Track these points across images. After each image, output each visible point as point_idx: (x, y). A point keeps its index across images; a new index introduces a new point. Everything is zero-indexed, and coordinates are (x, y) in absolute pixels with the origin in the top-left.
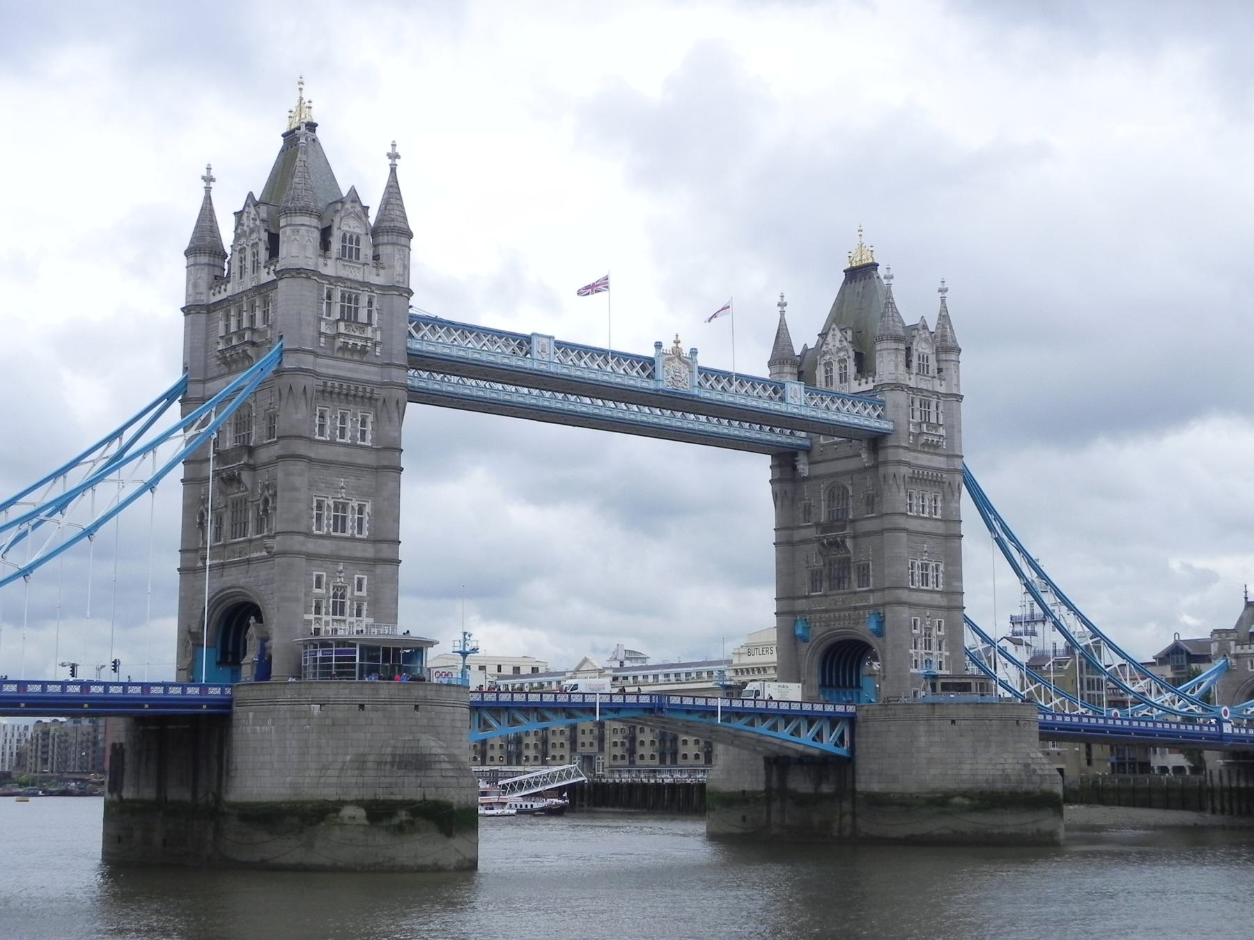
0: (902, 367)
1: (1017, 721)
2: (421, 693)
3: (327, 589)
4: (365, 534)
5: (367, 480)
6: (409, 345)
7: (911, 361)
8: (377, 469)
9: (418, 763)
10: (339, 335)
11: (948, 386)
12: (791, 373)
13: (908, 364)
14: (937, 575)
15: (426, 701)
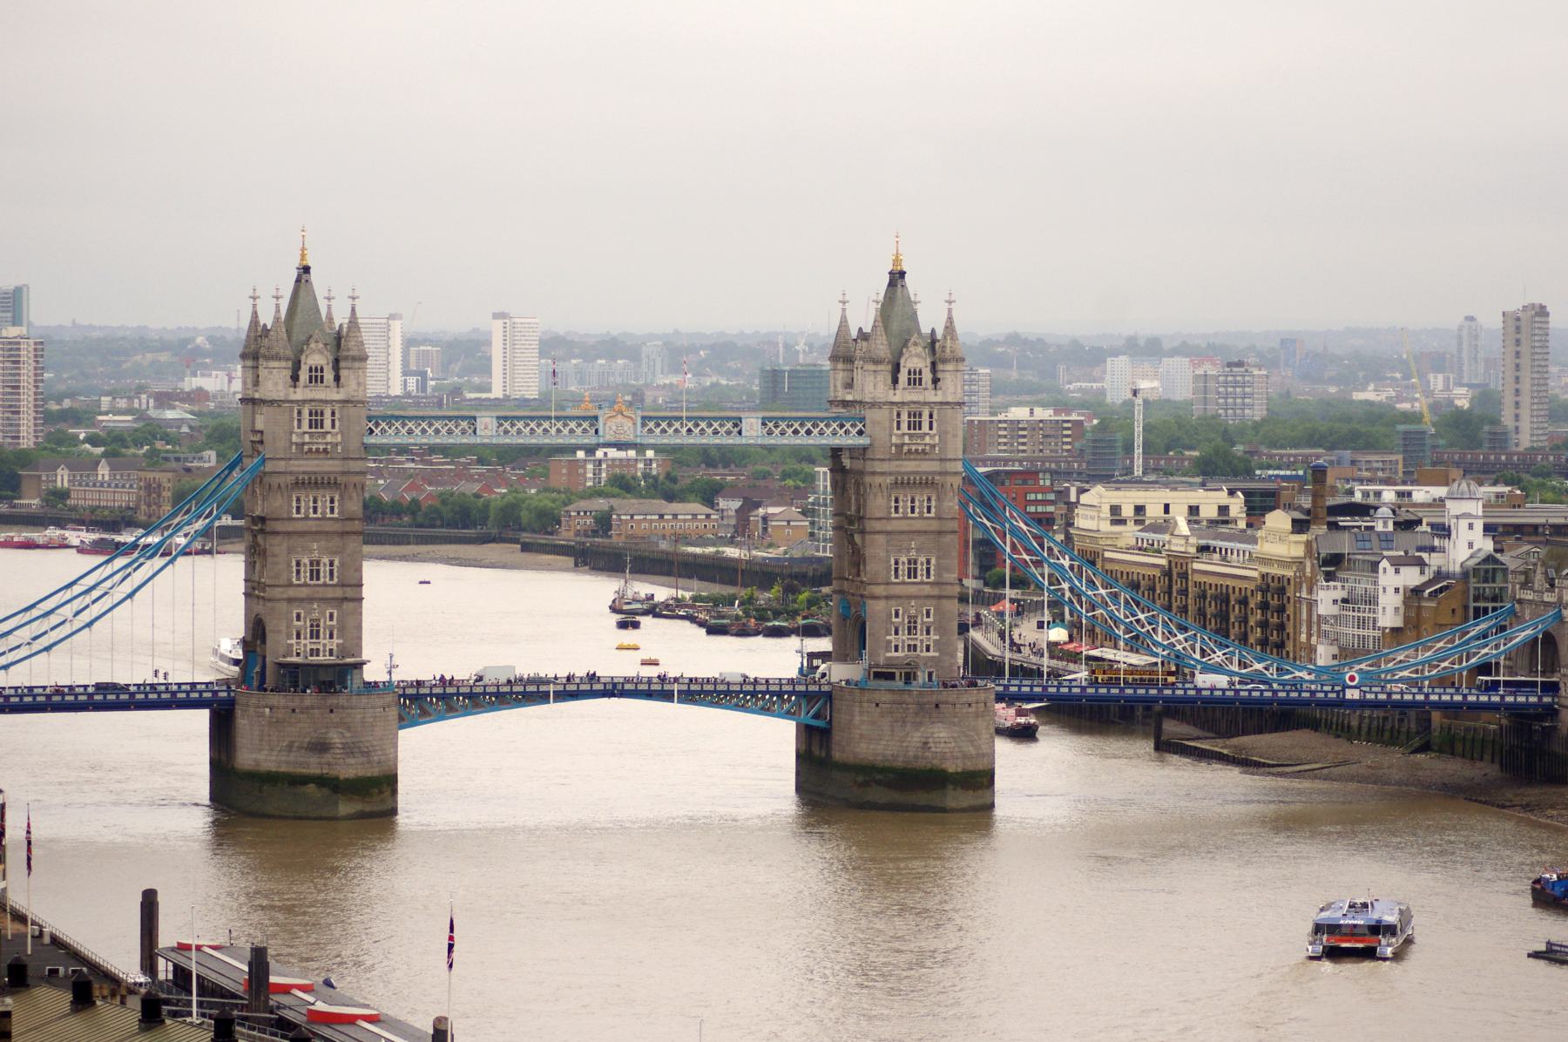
0: (881, 386)
1: (937, 706)
2: (335, 701)
3: (305, 622)
4: (336, 580)
5: (336, 541)
6: (365, 441)
7: (897, 378)
8: (343, 534)
9: (321, 747)
10: (304, 444)
11: (945, 394)
12: (844, 370)
13: (895, 381)
14: (928, 570)
15: (337, 707)
